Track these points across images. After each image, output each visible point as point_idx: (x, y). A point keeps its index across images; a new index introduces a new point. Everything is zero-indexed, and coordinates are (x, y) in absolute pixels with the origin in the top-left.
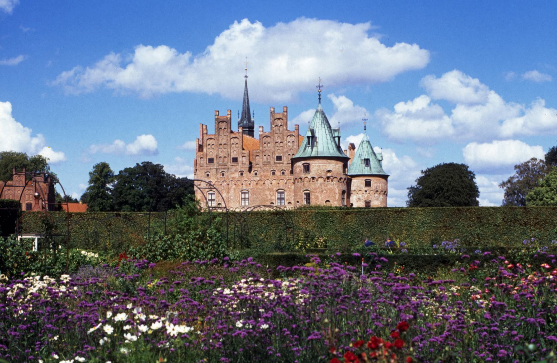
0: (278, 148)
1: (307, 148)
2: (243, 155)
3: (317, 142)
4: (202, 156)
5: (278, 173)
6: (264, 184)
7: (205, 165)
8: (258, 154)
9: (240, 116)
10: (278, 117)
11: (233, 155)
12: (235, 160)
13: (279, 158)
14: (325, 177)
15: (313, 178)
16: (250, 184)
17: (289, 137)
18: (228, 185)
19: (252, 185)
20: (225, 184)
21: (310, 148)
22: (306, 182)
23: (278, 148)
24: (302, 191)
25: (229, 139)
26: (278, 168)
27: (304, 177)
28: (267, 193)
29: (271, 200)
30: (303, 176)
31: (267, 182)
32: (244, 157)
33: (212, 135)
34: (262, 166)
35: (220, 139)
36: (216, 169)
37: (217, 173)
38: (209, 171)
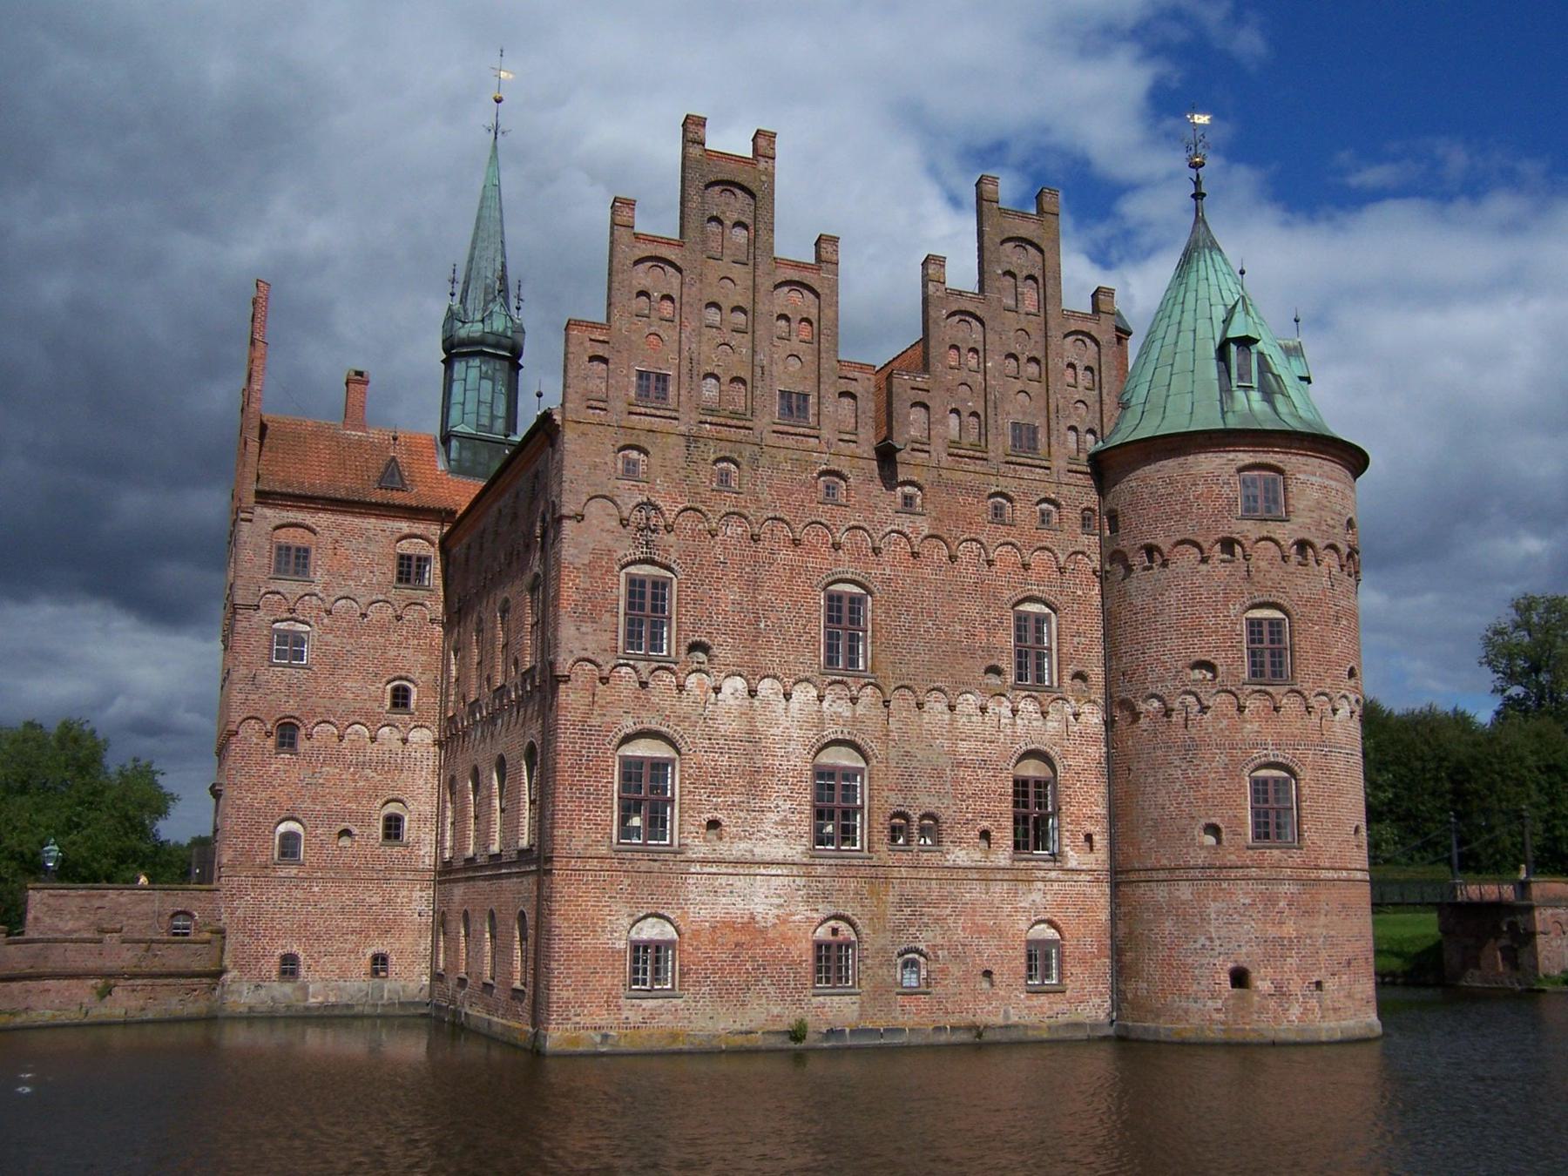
0: (1019, 385)
1: (1240, 394)
2: (844, 386)
3: (1277, 377)
4: (600, 350)
5: (1024, 512)
6: (953, 558)
7: (619, 405)
8: (922, 397)
9: (458, 289)
10: (1022, 233)
11: (788, 375)
12: (793, 404)
13: (1025, 437)
14: (1345, 550)
15: (1302, 545)
16: (876, 551)
17: (1071, 338)
18: (755, 538)
19: (886, 557)
20: (734, 530)
21: (1255, 396)
22: (1263, 564)
23: (1019, 385)
24: (1234, 609)
25: (765, 283)
26: (1025, 483)
27: (1253, 537)
28: (973, 609)
29: (989, 650)
30: (1249, 530)
31: (965, 551)
32: (846, 401)
33: (668, 242)
34: (946, 461)
35: (712, 277)
36: (691, 439)
37: (688, 458)
38: (643, 441)
